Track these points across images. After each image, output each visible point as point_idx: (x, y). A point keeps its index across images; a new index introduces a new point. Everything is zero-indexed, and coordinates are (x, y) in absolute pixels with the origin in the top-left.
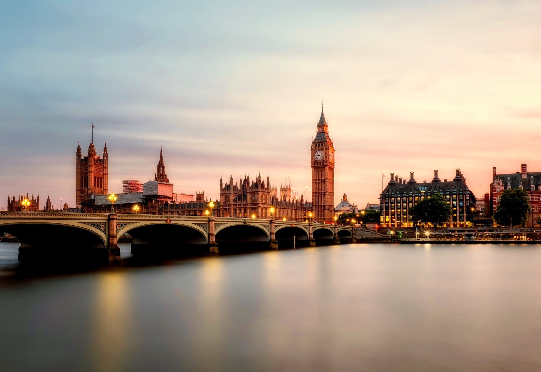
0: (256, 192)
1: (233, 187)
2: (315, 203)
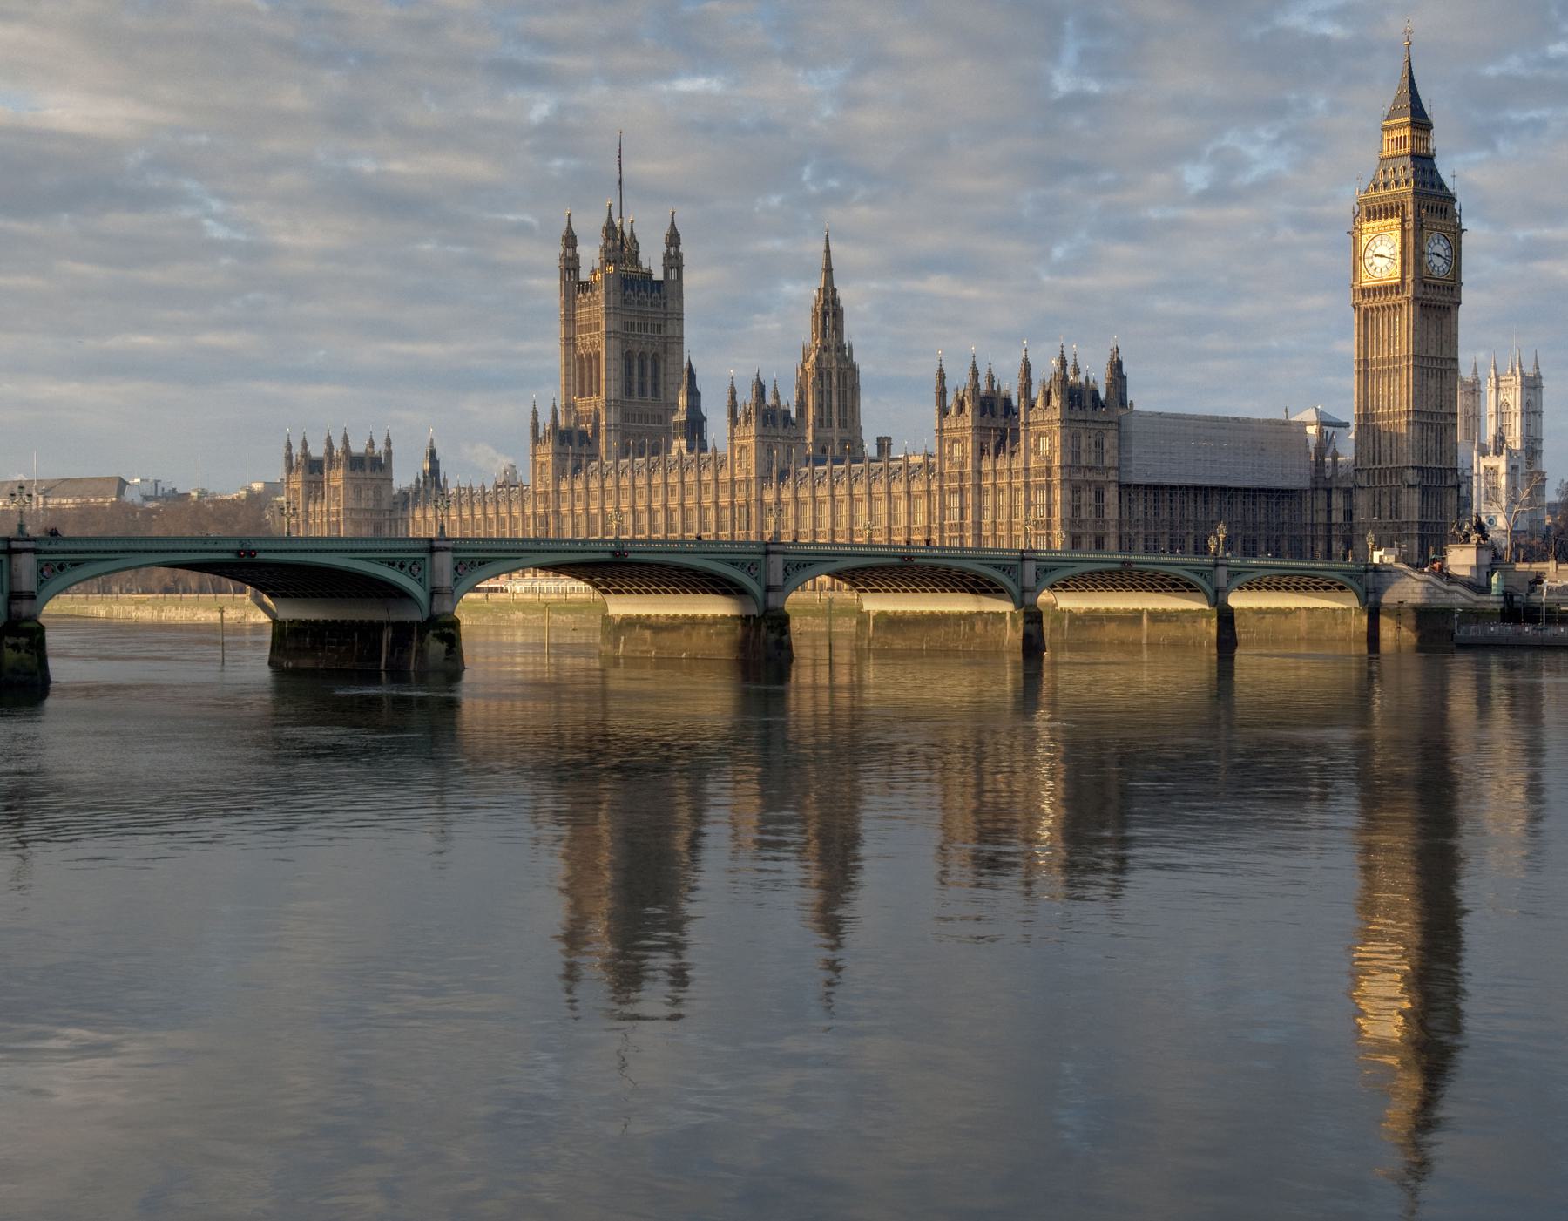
2: (1365, 460)
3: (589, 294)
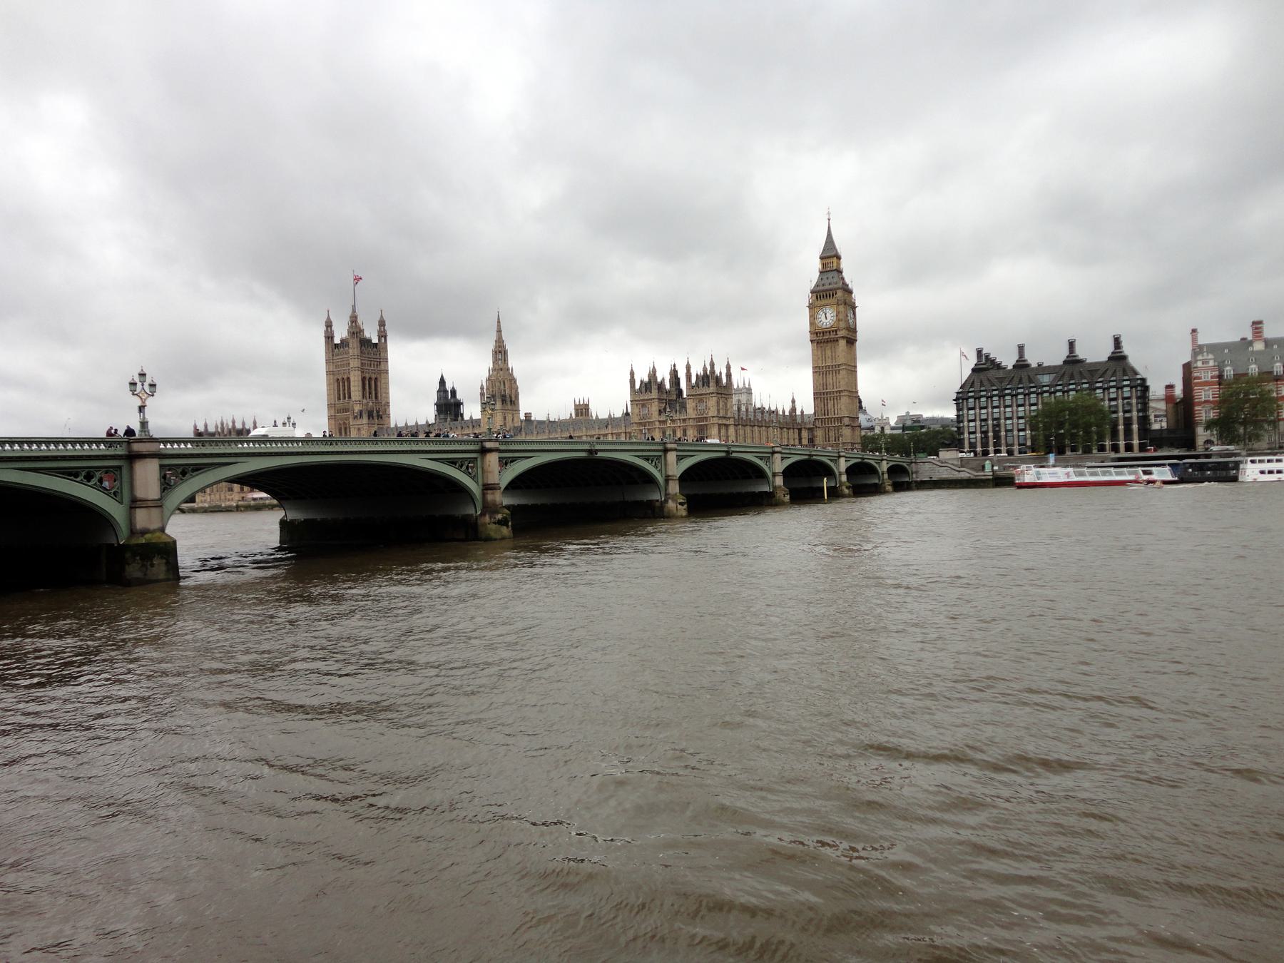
0: (705, 394)
1: (656, 387)
3: (342, 349)
